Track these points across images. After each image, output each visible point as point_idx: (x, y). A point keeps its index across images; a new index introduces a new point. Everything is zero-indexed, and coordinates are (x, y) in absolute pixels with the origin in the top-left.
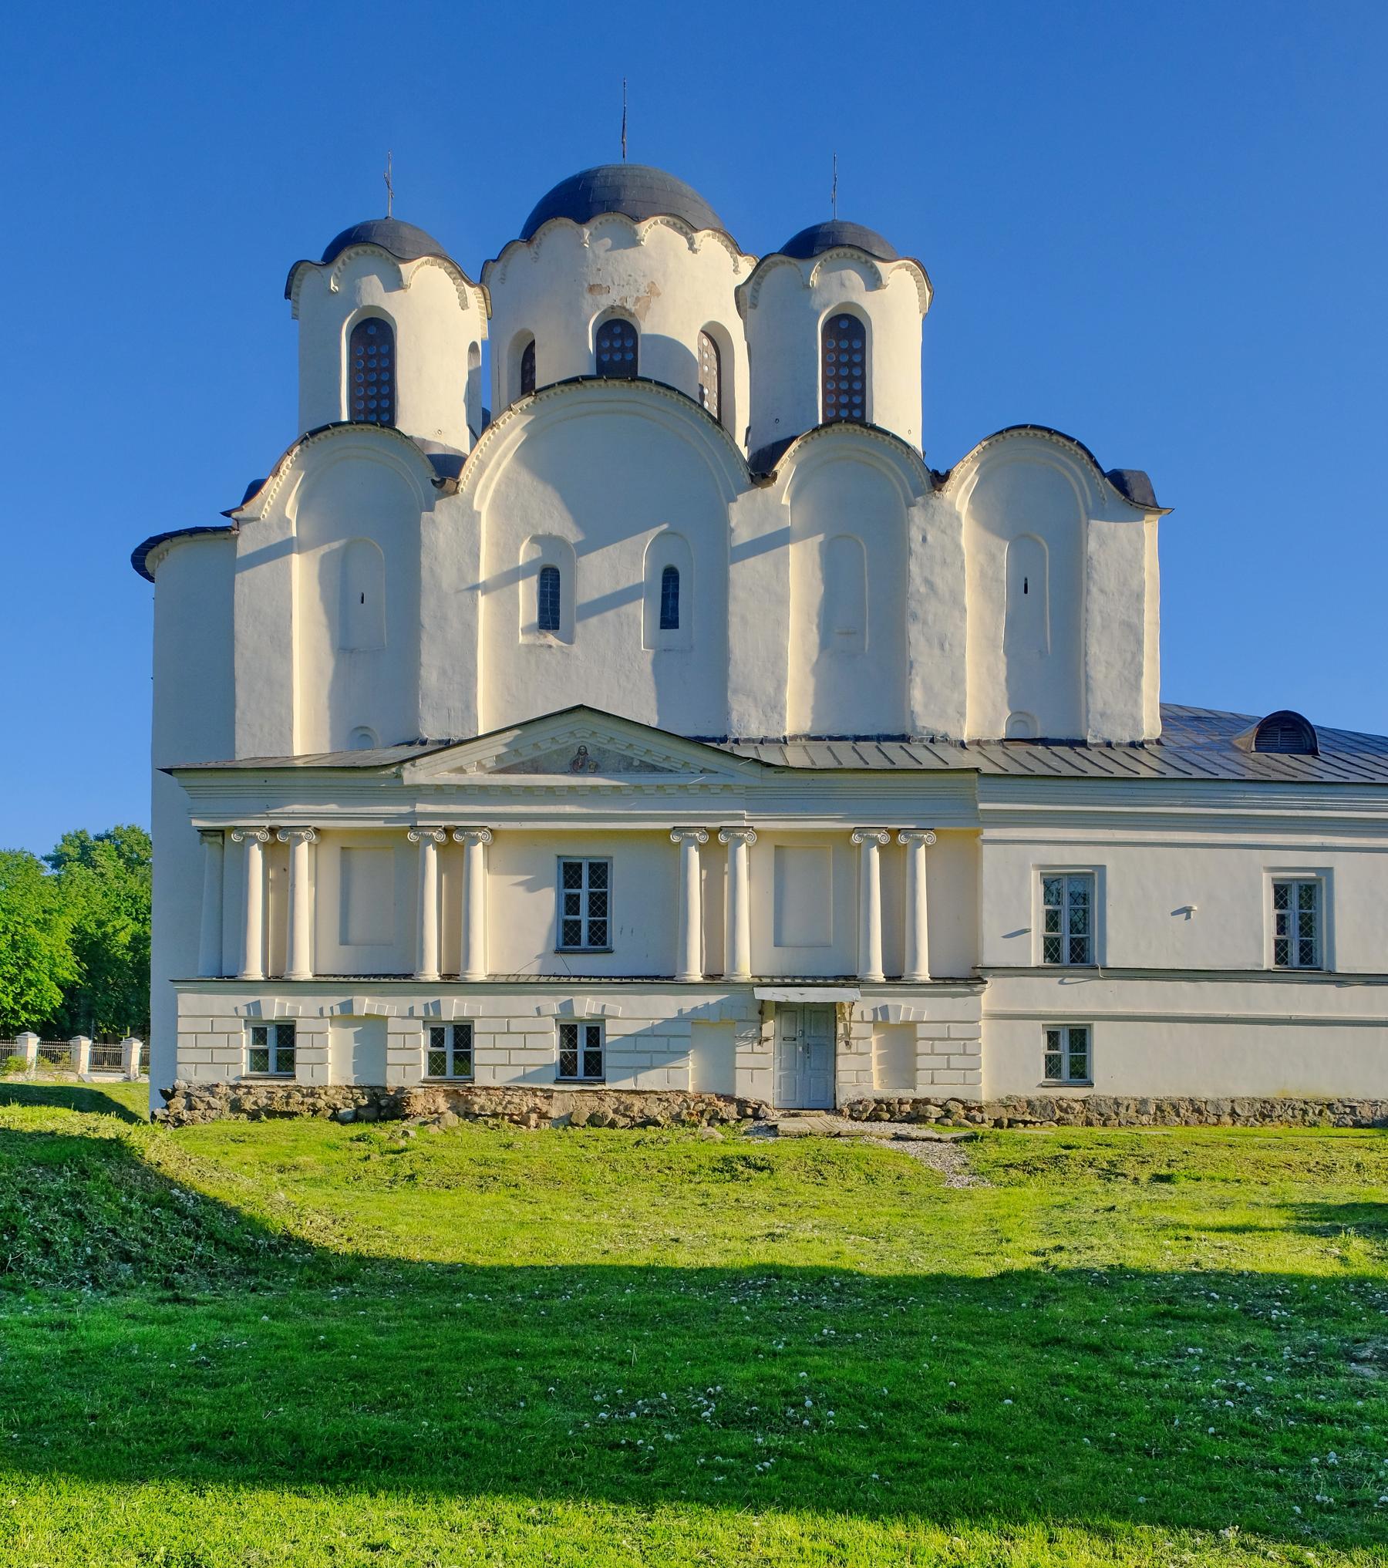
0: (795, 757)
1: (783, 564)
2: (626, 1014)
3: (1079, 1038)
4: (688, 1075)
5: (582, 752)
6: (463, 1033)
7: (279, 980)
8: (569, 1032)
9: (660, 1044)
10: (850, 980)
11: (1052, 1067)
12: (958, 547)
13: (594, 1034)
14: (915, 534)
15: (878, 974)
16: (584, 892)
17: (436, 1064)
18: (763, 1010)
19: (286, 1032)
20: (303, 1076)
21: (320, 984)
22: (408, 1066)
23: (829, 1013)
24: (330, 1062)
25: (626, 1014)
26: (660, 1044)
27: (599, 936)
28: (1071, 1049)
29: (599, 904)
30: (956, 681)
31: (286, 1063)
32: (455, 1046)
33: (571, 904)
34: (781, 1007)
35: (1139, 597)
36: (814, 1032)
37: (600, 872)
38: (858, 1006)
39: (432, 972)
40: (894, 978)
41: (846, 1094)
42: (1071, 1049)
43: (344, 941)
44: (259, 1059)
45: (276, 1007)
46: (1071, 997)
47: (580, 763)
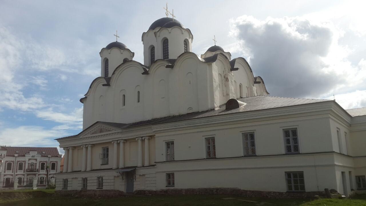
5: (101, 129)
46: (170, 168)
47: (101, 132)
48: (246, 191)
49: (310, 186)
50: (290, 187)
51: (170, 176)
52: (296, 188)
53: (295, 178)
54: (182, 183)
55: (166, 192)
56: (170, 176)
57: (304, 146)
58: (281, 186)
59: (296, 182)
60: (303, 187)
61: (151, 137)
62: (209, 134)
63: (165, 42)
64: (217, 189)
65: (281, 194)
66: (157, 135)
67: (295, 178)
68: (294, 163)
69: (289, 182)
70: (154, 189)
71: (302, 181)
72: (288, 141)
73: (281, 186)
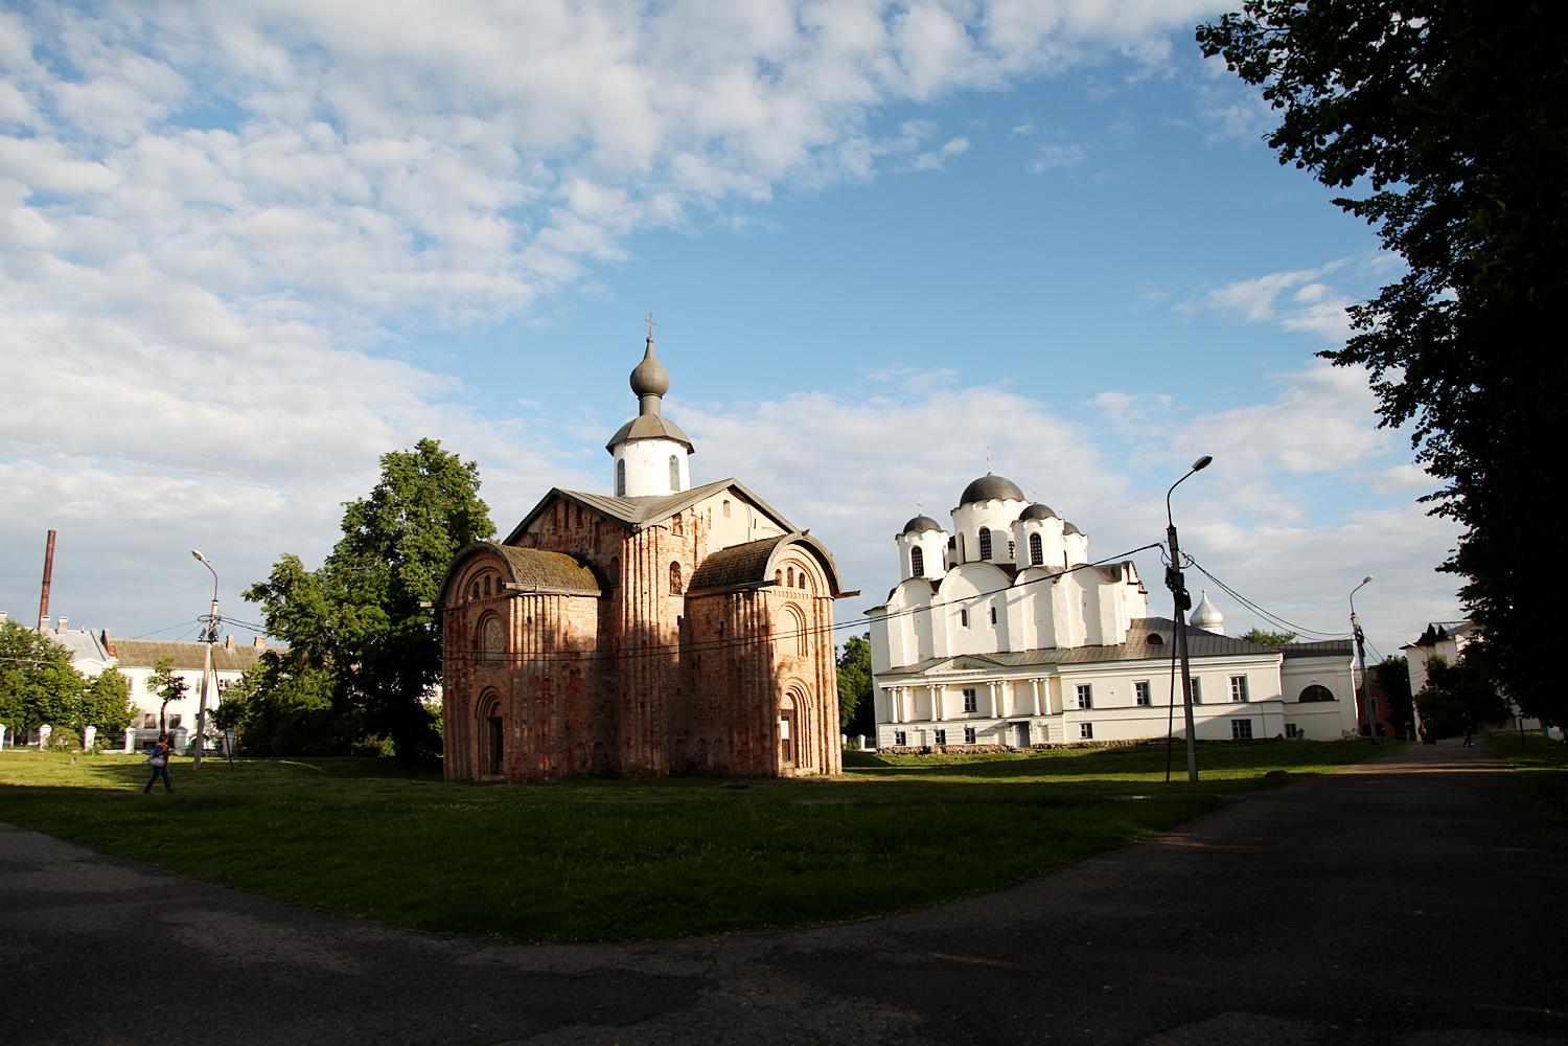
0: (1028, 659)
1: (1020, 604)
2: (979, 726)
3: (1089, 726)
4: (995, 740)
6: (943, 732)
7: (900, 722)
8: (967, 731)
9: (988, 733)
10: (1032, 715)
11: (1083, 734)
12: (1064, 597)
13: (973, 730)
14: (1053, 595)
15: (1038, 713)
16: (970, 697)
17: (938, 740)
18: (1011, 724)
19: (903, 734)
20: (908, 745)
21: (912, 722)
22: (931, 742)
23: (1027, 723)
24: (914, 741)
25: (979, 726)
26: (988, 733)
27: (974, 707)
29: (974, 700)
30: (1067, 632)
31: (904, 743)
32: (941, 736)
33: (967, 700)
34: (1016, 723)
35: (1114, 605)
36: (1024, 728)
37: (973, 692)
38: (1033, 722)
39: (935, 719)
40: (1042, 714)
41: (1032, 743)
43: (916, 712)
44: (898, 741)
45: (901, 728)
46: (1087, 716)
47: (965, 667)
49: (1257, 733)
50: (1235, 735)
51: (1087, 729)
52: (1242, 735)
55: (1081, 746)
56: (1087, 729)
58: (1228, 735)
59: (1242, 729)
60: (1250, 735)
61: (1055, 679)
63: (1036, 539)
66: (1062, 677)
69: (1235, 730)
71: (1249, 729)
73: (1228, 735)
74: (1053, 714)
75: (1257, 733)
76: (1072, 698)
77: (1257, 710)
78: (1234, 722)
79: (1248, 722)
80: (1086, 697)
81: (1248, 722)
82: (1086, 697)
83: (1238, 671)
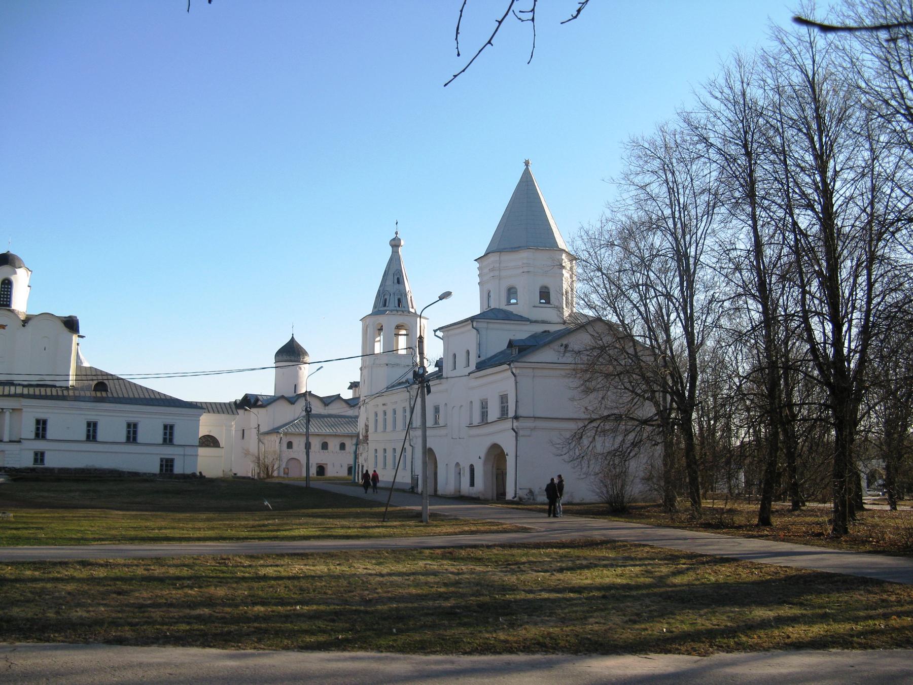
3: (42, 454)
11: (36, 461)
28: (39, 456)
42: (39, 456)
46: (40, 445)
48: (123, 472)
49: (178, 469)
50: (161, 470)
52: (166, 470)
53: (167, 464)
54: (52, 461)
55: (32, 470)
57: (177, 439)
58: (155, 468)
59: (167, 466)
60: (172, 470)
62: (92, 418)
64: (96, 470)
65: (155, 475)
67: (167, 464)
68: (168, 452)
69: (161, 466)
70: (17, 466)
71: (172, 466)
72: (165, 434)
73: (155, 468)
74: (10, 441)
75: (178, 469)
76: (29, 430)
77: (179, 451)
78: (162, 460)
79: (172, 460)
80: (41, 428)
81: (172, 460)
82: (41, 428)
83: (169, 421)
